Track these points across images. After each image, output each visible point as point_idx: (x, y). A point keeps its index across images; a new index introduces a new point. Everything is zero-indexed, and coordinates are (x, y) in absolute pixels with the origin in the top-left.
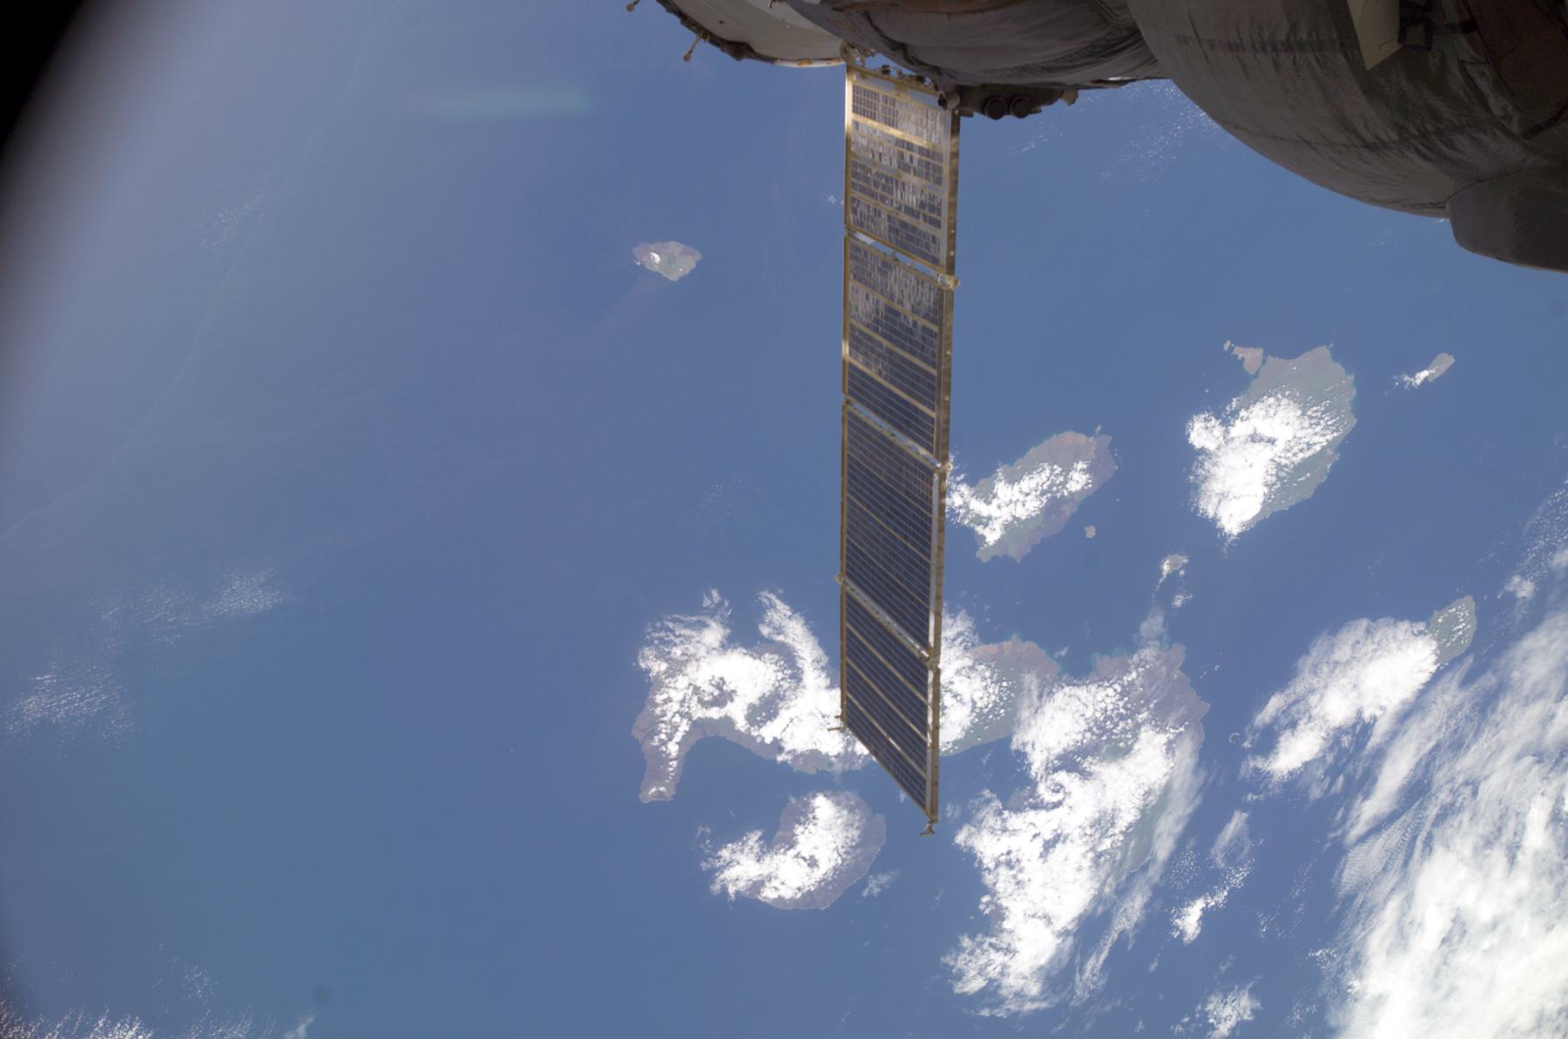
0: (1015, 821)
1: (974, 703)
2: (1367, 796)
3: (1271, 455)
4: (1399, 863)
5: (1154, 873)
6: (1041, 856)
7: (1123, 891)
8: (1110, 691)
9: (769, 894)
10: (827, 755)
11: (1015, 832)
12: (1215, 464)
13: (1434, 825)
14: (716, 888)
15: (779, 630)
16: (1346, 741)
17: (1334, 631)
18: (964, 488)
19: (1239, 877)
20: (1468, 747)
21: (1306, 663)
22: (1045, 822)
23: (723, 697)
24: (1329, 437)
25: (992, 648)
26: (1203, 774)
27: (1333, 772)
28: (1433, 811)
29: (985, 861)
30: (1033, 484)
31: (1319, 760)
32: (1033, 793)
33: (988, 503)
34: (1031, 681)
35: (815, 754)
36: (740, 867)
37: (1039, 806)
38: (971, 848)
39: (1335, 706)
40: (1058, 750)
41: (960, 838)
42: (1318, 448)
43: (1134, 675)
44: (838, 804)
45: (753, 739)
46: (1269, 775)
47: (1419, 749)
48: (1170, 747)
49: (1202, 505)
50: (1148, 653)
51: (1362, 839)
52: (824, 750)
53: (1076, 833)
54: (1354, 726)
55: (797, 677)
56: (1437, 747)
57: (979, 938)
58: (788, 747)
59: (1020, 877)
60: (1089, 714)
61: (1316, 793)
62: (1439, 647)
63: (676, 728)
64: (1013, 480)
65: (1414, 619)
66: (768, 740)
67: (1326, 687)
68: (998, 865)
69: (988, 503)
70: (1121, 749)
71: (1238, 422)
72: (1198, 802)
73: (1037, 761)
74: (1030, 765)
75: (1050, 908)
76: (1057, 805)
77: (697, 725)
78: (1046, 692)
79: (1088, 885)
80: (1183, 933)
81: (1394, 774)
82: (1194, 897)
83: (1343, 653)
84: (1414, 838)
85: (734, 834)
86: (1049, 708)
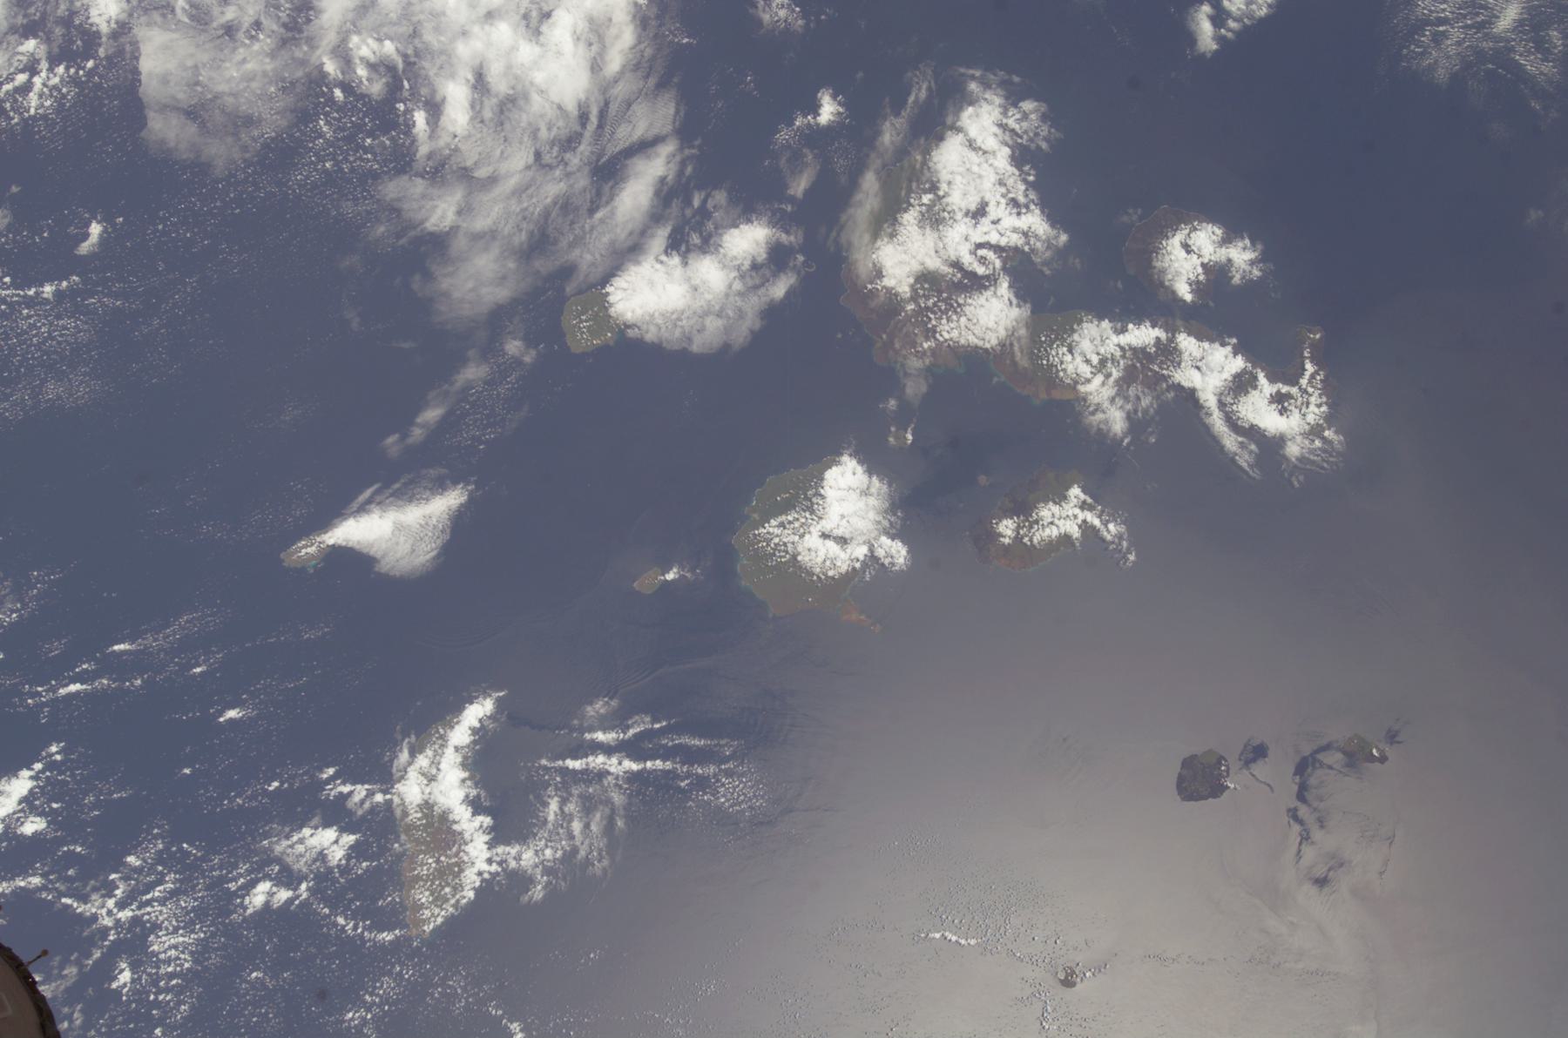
0: (1016, 240)
1: (1070, 351)
2: (662, 180)
3: (823, 522)
4: (613, 108)
5: (875, 162)
6: (987, 204)
7: (902, 152)
8: (946, 336)
9: (1219, 232)
11: (1015, 230)
12: (879, 523)
13: (581, 135)
14: (1259, 247)
16: (695, 239)
17: (726, 347)
18: (1109, 538)
19: (783, 136)
20: (555, 203)
21: (751, 322)
23: (1279, 400)
25: (1057, 395)
26: (843, 240)
27: (704, 213)
28: (585, 148)
29: (1037, 211)
30: (1048, 531)
31: (720, 228)
32: (1004, 262)
33: (1084, 521)
34: (1023, 361)
35: (1200, 338)
36: (1241, 256)
37: (997, 248)
38: (1053, 226)
40: (989, 293)
41: (1064, 238)
42: (774, 523)
43: (926, 345)
44: (1174, 293)
45: (1247, 360)
46: (773, 223)
47: (613, 213)
48: (879, 273)
49: (885, 488)
50: (915, 364)
52: (1192, 340)
53: (959, 216)
54: (688, 250)
55: (1222, 405)
56: (592, 211)
57: (1033, 146)
58: (1229, 348)
59: (1003, 190)
60: (963, 319)
61: (720, 197)
62: (606, 309)
63: (1310, 382)
64: (1066, 538)
65: (639, 344)
66: (1239, 357)
67: (727, 295)
68: (1027, 207)
69: (1084, 521)
70: (926, 281)
71: (862, 558)
72: (844, 218)
73: (1004, 287)
74: (1010, 287)
75: (973, 156)
76: (980, 246)
77: (1294, 381)
78: (1005, 347)
79: (939, 166)
80: (834, 97)
81: (635, 195)
82: (829, 129)
83: (713, 324)
84: (600, 126)
85: (1250, 286)
86: (1002, 333)
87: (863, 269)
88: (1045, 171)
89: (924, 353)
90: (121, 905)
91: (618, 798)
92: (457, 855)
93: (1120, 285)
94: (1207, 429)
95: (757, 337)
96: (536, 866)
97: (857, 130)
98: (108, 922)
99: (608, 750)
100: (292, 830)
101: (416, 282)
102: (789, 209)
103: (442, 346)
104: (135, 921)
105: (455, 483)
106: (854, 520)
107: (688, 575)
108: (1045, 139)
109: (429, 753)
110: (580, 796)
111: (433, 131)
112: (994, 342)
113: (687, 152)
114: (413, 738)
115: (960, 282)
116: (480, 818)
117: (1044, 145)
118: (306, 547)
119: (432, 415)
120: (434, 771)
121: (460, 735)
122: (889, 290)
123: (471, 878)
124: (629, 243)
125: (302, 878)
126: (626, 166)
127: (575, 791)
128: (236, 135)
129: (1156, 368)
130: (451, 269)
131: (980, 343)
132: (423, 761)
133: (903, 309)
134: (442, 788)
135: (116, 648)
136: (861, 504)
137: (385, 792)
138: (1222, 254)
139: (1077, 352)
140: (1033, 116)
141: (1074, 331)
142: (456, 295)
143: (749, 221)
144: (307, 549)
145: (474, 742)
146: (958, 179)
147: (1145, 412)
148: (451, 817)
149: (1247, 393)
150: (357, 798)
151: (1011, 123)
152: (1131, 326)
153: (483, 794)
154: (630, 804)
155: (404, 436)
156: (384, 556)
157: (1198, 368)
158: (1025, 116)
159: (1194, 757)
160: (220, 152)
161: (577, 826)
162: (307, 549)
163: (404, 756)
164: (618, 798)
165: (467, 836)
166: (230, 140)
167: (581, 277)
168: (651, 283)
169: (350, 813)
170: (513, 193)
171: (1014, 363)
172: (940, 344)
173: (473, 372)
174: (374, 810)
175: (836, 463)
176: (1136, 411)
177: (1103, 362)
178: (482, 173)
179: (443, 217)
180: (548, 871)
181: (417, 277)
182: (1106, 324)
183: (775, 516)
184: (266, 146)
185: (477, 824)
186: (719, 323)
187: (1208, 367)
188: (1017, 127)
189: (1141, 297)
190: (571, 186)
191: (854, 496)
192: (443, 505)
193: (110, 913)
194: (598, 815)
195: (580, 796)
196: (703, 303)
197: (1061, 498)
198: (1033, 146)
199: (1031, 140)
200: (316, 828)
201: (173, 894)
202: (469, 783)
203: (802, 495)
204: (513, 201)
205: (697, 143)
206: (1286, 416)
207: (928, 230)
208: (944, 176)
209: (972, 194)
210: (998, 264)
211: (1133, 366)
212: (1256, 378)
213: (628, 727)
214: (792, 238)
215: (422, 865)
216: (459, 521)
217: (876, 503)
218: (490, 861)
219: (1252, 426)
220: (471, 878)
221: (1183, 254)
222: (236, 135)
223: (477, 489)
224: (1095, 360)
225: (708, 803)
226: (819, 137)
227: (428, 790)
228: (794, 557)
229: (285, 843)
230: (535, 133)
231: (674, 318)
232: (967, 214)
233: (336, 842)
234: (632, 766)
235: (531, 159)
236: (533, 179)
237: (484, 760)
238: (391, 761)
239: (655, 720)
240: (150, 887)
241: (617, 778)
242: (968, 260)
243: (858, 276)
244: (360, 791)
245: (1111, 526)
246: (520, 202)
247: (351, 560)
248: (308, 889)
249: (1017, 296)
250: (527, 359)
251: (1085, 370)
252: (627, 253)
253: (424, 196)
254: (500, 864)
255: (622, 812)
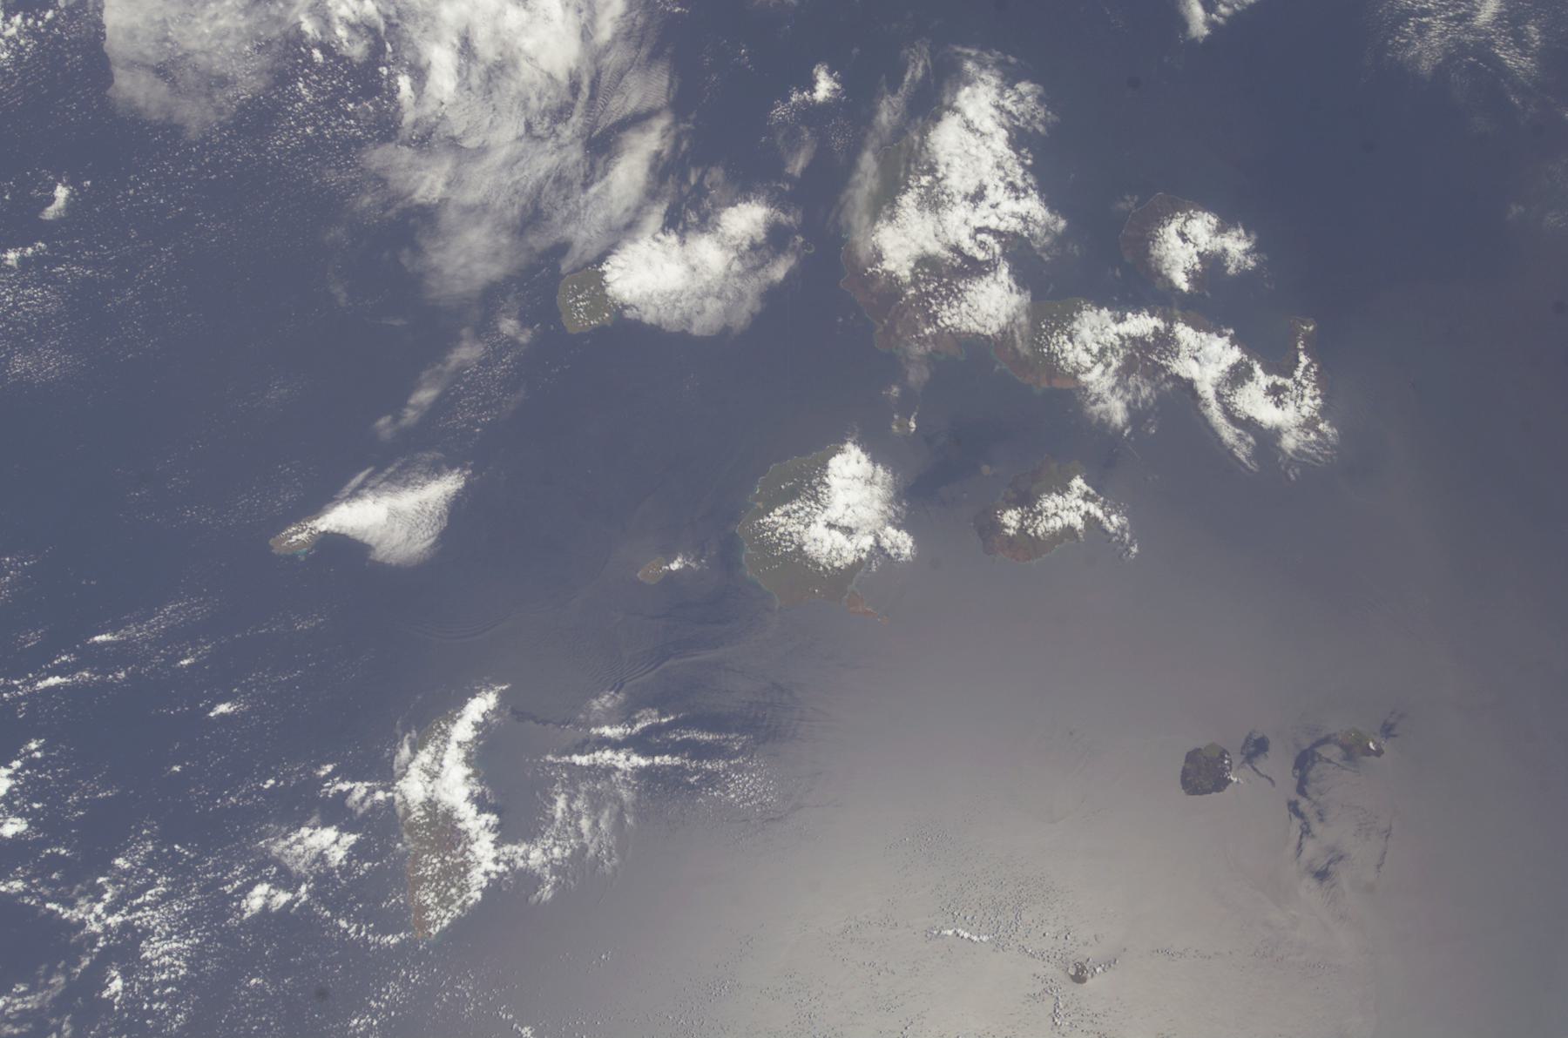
0: (1014, 225)
1: (1070, 339)
2: (657, 155)
3: (828, 512)
5: (873, 142)
6: (985, 187)
7: (899, 132)
8: (948, 322)
9: (1214, 221)
10: (1187, 324)
11: (1013, 215)
12: (884, 512)
13: (573, 105)
14: (1253, 237)
15: (1240, 438)
16: (693, 217)
17: (726, 330)
18: (1112, 529)
19: (779, 112)
20: (548, 177)
21: (751, 304)
22: (983, 216)
23: (1275, 392)
24: (767, 519)
25: (1057, 384)
27: (700, 191)
28: (577, 120)
30: (1052, 522)
33: (1087, 513)
34: (1024, 349)
35: (1197, 328)
36: (1236, 245)
37: (997, 233)
38: (1051, 211)
39: (711, 255)
40: (989, 279)
41: (1062, 224)
42: (778, 511)
43: (927, 331)
44: (1171, 282)
45: (1244, 351)
46: (770, 203)
47: (607, 187)
48: (879, 256)
50: (917, 350)
51: (651, 114)
52: (1190, 330)
53: (958, 199)
54: (686, 229)
55: (1219, 396)
56: (586, 186)
57: (1030, 129)
58: (1226, 339)
59: (1001, 173)
60: (964, 305)
61: (717, 174)
62: (603, 288)
64: (1069, 530)
65: (638, 324)
66: (1236, 348)
67: (726, 276)
68: (1025, 191)
69: (1087, 513)
71: (867, 548)
72: (843, 198)
73: (1004, 272)
74: (1010, 273)
75: (970, 137)
76: (979, 230)
77: (1289, 375)
78: (1006, 333)
79: (938, 148)
81: (628, 173)
82: (825, 106)
83: (713, 306)
84: (592, 97)
85: (1244, 276)
86: (1003, 320)
87: (864, 251)
88: (1044, 155)
89: (926, 339)
90: (111, 910)
91: (626, 795)
92: (462, 854)
93: (1118, 273)
94: (1206, 420)
95: (757, 320)
96: (545, 865)
97: (854, 107)
98: (96, 928)
99: (615, 745)
100: (290, 830)
101: (405, 257)
102: (787, 187)
103: (435, 325)
104: (126, 927)
105: (451, 468)
106: (860, 510)
107: (693, 565)
108: (1042, 122)
109: (431, 749)
110: (588, 793)
111: (418, 97)
112: (995, 329)
113: (682, 126)
114: (414, 733)
115: (960, 267)
116: (486, 816)
117: (1041, 129)
118: (297, 533)
119: (425, 396)
120: (437, 768)
121: (462, 731)
122: (889, 274)
123: (477, 878)
124: (626, 220)
125: (301, 879)
126: (619, 140)
127: (583, 787)
128: (209, 95)
129: (1155, 358)
130: (441, 243)
131: (981, 330)
132: (425, 757)
133: (903, 293)
134: (446, 785)
135: (97, 638)
136: (866, 494)
137: (386, 790)
138: (1218, 243)
139: (1077, 340)
140: (1029, 98)
141: (1074, 319)
142: (448, 270)
143: (747, 200)
144: (298, 536)
145: (477, 738)
146: (957, 161)
147: (1145, 402)
148: (455, 815)
149: (1243, 384)
150: (357, 796)
151: (1008, 104)
152: (1129, 315)
153: (488, 792)
154: (638, 801)
155: (396, 419)
156: (378, 544)
157: (1196, 359)
158: (1022, 98)
159: (1198, 750)
160: (194, 114)
161: (585, 824)
162: (298, 536)
163: (405, 752)
164: (626, 795)
165: (472, 835)
166: (203, 100)
167: (577, 255)
168: (649, 263)
169: (351, 812)
170: (505, 164)
171: (1016, 351)
172: (941, 331)
173: (467, 352)
174: (375, 807)
175: (839, 450)
176: (1136, 401)
177: (1103, 351)
178: (471, 143)
179: (431, 189)
180: (555, 870)
181: (406, 251)
182: (1105, 312)
183: (780, 504)
184: (241, 108)
185: (482, 822)
186: (719, 304)
187: (1206, 358)
188: (1013, 109)
189: (1138, 285)
190: (564, 159)
191: (859, 485)
192: (439, 490)
193: (98, 918)
194: (607, 813)
195: (588, 793)
196: (701, 284)
197: (1064, 489)
198: (1030, 129)
199: (1028, 123)
200: (315, 828)
201: (165, 898)
202: (473, 780)
203: (806, 484)
204: (504, 174)
205: (693, 116)
206: (1281, 408)
207: (927, 213)
208: (942, 157)
209: (973, 176)
210: (998, 249)
211: (1133, 356)
212: (1251, 370)
213: (635, 722)
214: (791, 218)
215: (426, 865)
216: (457, 507)
217: (881, 492)
218: (496, 861)
219: (1249, 418)
220: (477, 878)
221: (1179, 242)
222: (209, 95)
223: (473, 474)
224: (1095, 349)
225: (719, 798)
226: (815, 114)
227: (430, 787)
228: (800, 547)
229: (283, 843)
230: (525, 105)
231: (674, 298)
232: (965, 197)
233: (336, 842)
234: (643, 762)
235: (522, 130)
236: (524, 150)
237: (487, 756)
238: (392, 758)
239: (662, 714)
240: (141, 891)
241: (625, 774)
242: (967, 245)
243: (858, 259)
244: (360, 789)
245: (1114, 518)
246: (511, 174)
247: (345, 551)
248: (308, 891)
249: (1017, 283)
250: (523, 339)
251: (1086, 359)
252: (625, 230)
253: (410, 166)
254: (507, 863)
255: (631, 809)
